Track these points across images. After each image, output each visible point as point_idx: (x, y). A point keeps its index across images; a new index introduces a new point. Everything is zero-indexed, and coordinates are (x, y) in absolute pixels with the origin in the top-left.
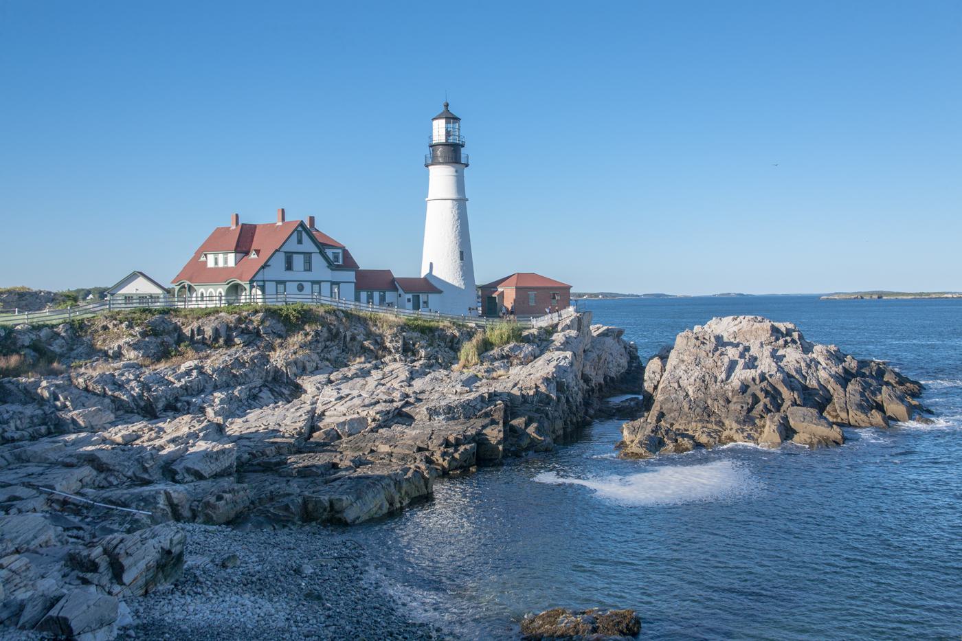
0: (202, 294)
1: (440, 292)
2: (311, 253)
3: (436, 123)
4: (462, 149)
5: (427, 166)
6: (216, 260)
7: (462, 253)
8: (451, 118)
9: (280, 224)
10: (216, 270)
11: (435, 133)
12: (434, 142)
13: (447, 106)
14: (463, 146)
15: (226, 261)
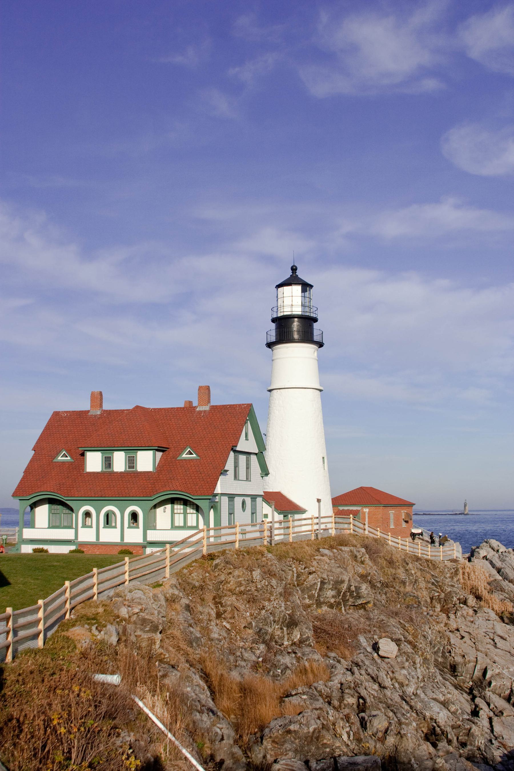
0: (88, 514)
1: (303, 511)
2: (249, 454)
3: (287, 289)
4: (315, 325)
5: (270, 345)
6: (108, 462)
7: (323, 458)
8: (306, 287)
9: (207, 408)
10: (107, 476)
11: (287, 301)
12: (280, 315)
13: (294, 269)
14: (315, 320)
15: (131, 462)
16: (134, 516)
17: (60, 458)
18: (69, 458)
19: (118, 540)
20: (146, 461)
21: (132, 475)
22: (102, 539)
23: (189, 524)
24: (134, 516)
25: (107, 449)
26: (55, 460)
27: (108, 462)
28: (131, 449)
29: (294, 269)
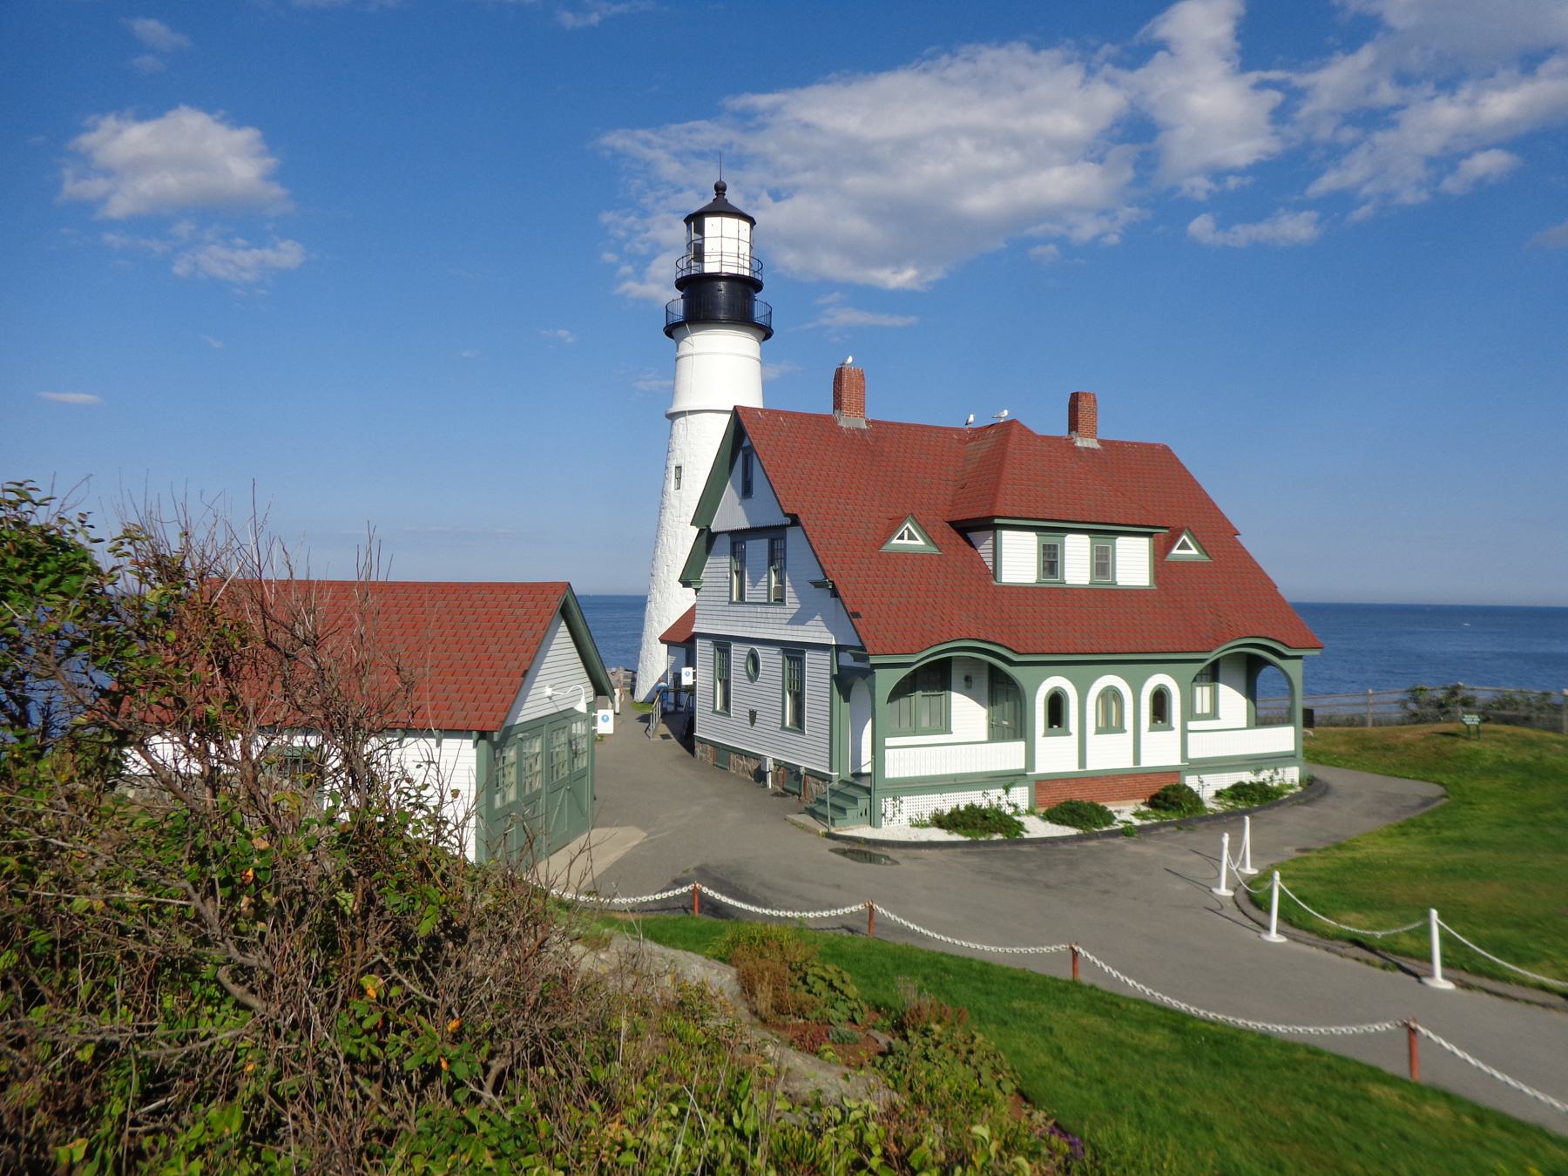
6: (1051, 561)
10: (1050, 593)
13: (720, 189)
16: (1160, 701)
17: (895, 541)
18: (1194, 552)
19: (1127, 763)
20: (1133, 562)
21: (1103, 596)
22: (1093, 765)
23: (1198, 711)
24: (1160, 701)
25: (1051, 528)
26: (886, 548)
27: (1051, 561)
28: (1104, 530)
29: (720, 189)
